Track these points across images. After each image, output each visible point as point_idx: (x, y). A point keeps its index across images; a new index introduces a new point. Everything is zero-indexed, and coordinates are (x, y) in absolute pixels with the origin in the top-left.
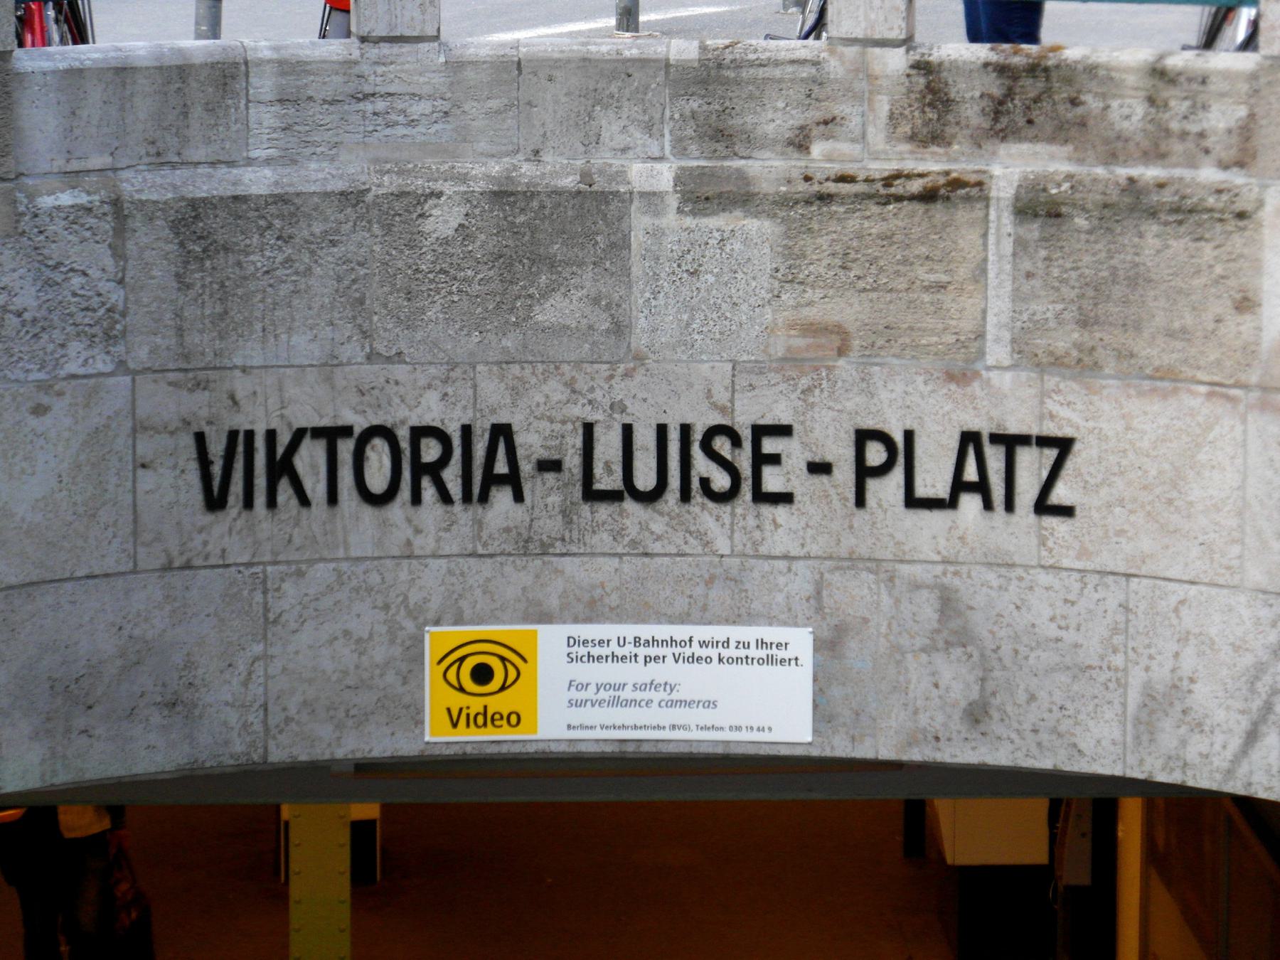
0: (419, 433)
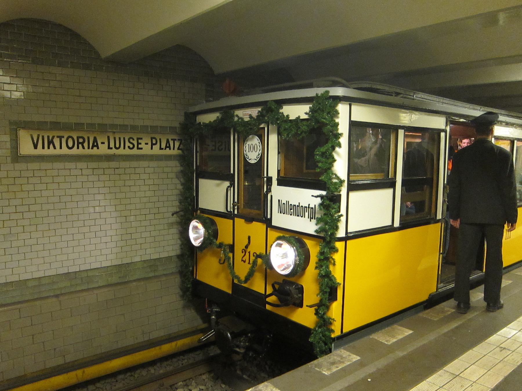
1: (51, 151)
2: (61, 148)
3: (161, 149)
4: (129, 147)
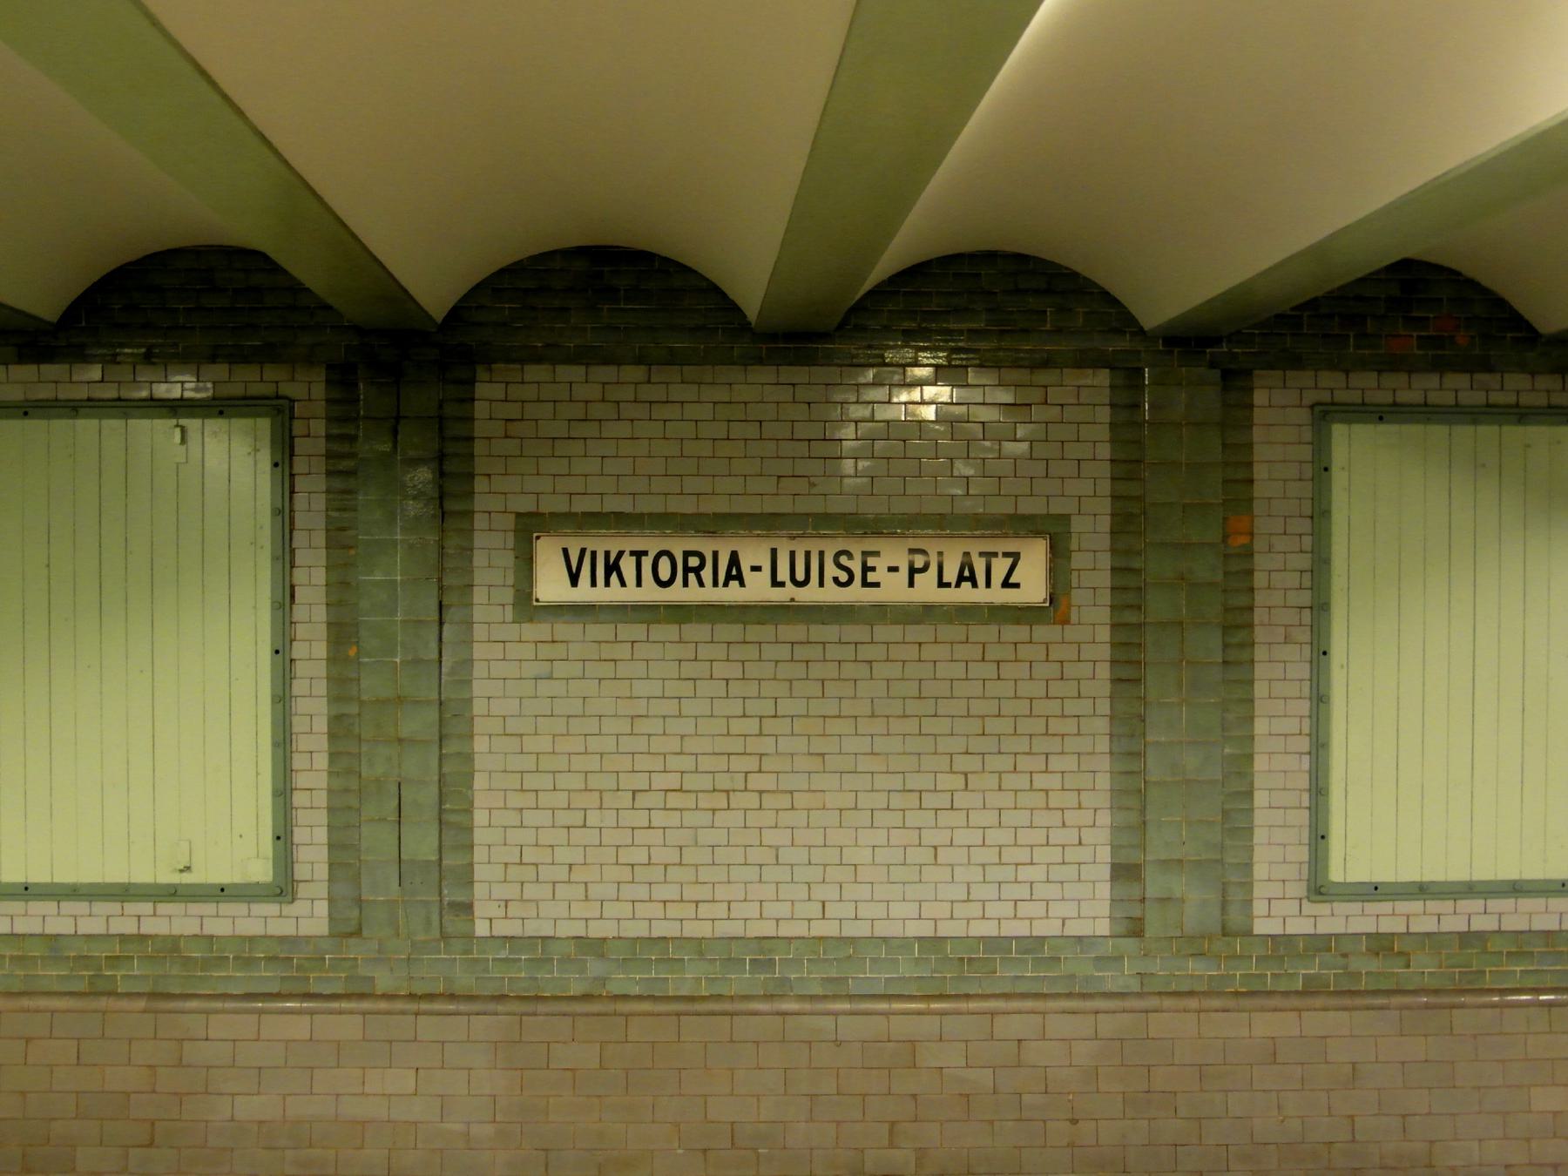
0: (687, 554)
1: (613, 594)
2: (639, 584)
3: (942, 584)
4: (836, 580)
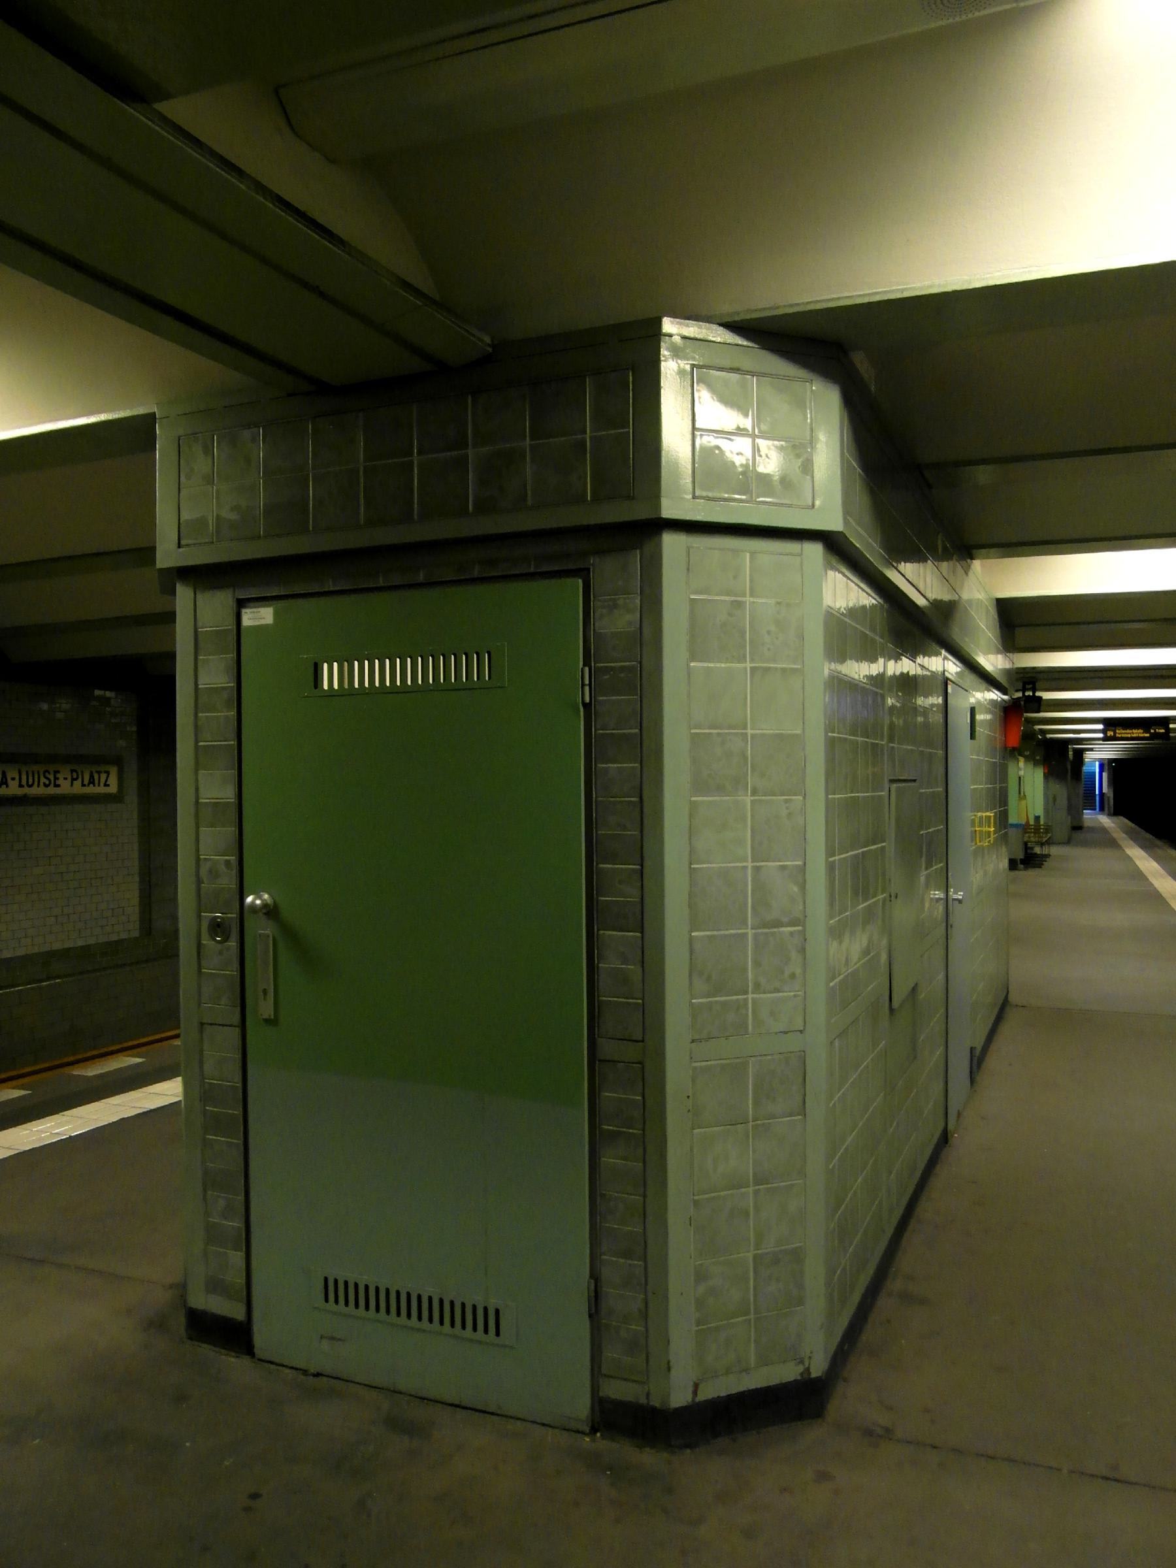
3: (83, 785)
